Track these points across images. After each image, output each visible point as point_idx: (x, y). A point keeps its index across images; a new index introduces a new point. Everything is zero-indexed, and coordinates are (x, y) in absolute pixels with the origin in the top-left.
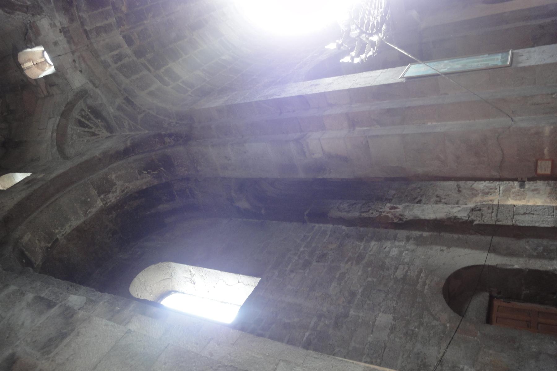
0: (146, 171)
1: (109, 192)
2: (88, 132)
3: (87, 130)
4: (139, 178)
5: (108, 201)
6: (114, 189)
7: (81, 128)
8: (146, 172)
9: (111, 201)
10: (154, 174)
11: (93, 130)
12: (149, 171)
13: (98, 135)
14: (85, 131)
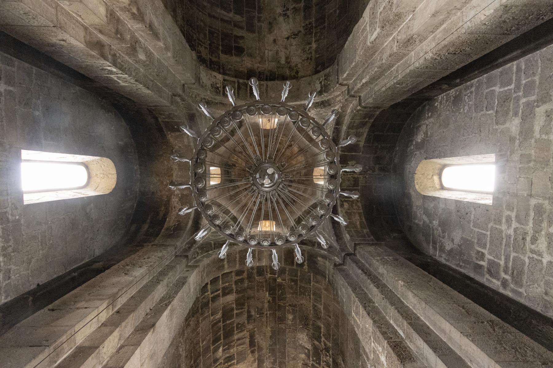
1: (179, 200)
5: (175, 197)
6: (179, 203)
9: (174, 198)
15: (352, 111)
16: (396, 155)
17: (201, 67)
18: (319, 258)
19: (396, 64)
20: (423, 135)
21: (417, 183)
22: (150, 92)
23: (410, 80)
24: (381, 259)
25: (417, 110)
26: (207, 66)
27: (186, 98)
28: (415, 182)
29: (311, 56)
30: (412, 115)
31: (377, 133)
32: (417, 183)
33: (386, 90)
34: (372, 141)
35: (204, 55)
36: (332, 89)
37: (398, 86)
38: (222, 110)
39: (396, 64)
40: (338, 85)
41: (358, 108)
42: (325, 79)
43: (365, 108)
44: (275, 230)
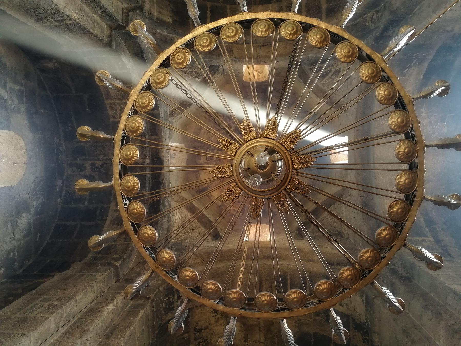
0: (406, 68)
2: (332, 75)
3: (330, 75)
4: (407, 78)
7: (326, 78)
8: (407, 69)
10: (414, 64)
11: (333, 70)
12: (407, 67)
13: (340, 69)
14: (331, 77)
15: (129, 257)
16: (61, 191)
17: (363, 319)
18: (169, 20)
19: (61, 336)
20: (19, 222)
21: (23, 150)
22: (451, 287)
23: (36, 313)
24: (63, 20)
25: (31, 261)
26: (354, 320)
27: (388, 274)
28: (25, 151)
29: (195, 334)
30: (39, 252)
31: (91, 223)
32: (22, 149)
33: (74, 295)
34: (98, 211)
35: (359, 337)
36: (161, 289)
37: (56, 303)
38: (330, 254)
39: (61, 337)
40: (152, 296)
41: (120, 262)
42: (173, 303)
43: (109, 264)
44: (245, 67)
